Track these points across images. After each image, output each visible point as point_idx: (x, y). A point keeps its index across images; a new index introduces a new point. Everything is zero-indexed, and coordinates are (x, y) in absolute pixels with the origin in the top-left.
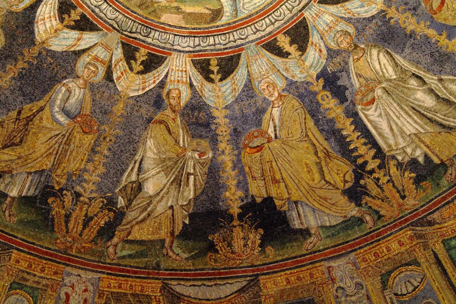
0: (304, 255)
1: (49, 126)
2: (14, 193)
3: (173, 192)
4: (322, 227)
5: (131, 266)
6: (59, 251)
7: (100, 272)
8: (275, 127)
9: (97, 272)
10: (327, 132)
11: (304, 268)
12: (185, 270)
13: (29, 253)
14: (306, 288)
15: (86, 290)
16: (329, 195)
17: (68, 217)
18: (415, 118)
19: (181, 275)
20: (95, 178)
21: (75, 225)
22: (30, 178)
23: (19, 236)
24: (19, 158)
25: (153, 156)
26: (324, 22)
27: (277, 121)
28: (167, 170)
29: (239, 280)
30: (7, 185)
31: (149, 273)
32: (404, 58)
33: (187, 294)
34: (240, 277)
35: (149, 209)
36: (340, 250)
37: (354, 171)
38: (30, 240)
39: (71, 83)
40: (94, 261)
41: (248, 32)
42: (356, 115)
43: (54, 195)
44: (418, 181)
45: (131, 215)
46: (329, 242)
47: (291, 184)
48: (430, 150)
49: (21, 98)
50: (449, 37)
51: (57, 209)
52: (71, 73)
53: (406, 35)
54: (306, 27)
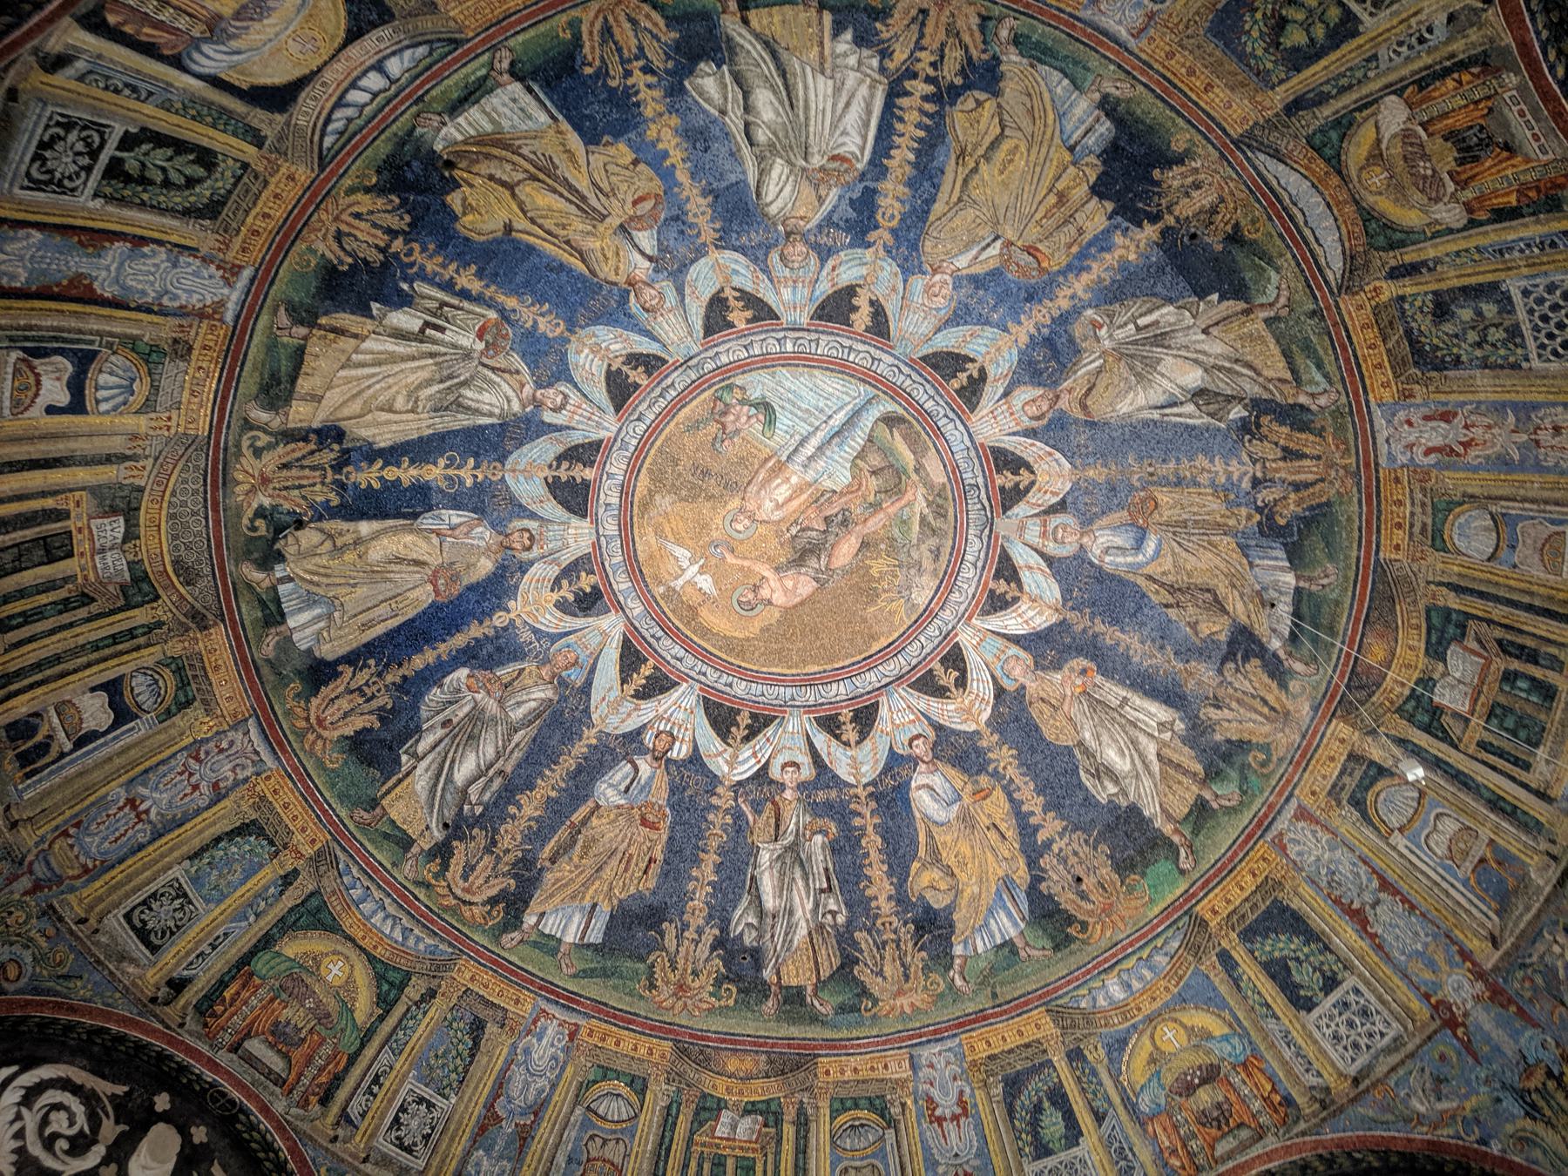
0: (1146, 86)
1: (1170, 559)
2: (1289, 579)
3: (1180, 339)
4: (1077, 87)
5: (1337, 359)
6: (1359, 484)
7: (1368, 407)
8: (984, 249)
9: (1369, 412)
10: (931, 178)
11: (1169, 75)
12: (1298, 265)
13: (1378, 531)
14: (1197, 53)
15: (1410, 423)
16: (1020, 110)
17: (1297, 487)
18: (801, 93)
19: (1310, 269)
20: (1218, 466)
21: (1308, 471)
22: (1258, 562)
23: (1354, 554)
24: (1234, 586)
25: (1141, 394)
26: (794, 294)
27: (974, 252)
28: (1152, 364)
29: (1261, 168)
30: (1280, 593)
31: (1335, 324)
32: (744, 172)
33: (1338, 245)
34: (1255, 168)
35: (1227, 365)
36: (1089, 36)
37: (953, 104)
38: (1356, 534)
39: (1095, 553)
40: (1353, 422)
41: (885, 365)
42: (871, 162)
43: (1270, 517)
44: (883, 14)
45: (1252, 390)
46: (1094, 61)
47: (1050, 173)
48: (822, 37)
49: (1146, 611)
50: (665, 155)
51: (1292, 507)
52: (1081, 556)
53: (716, 197)
54: (822, 307)
